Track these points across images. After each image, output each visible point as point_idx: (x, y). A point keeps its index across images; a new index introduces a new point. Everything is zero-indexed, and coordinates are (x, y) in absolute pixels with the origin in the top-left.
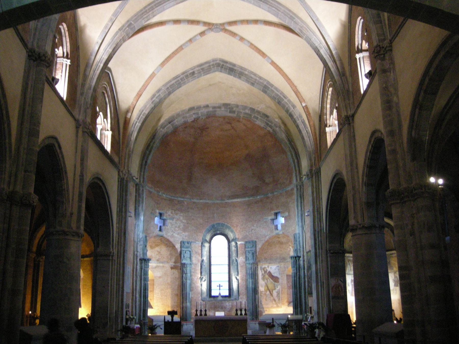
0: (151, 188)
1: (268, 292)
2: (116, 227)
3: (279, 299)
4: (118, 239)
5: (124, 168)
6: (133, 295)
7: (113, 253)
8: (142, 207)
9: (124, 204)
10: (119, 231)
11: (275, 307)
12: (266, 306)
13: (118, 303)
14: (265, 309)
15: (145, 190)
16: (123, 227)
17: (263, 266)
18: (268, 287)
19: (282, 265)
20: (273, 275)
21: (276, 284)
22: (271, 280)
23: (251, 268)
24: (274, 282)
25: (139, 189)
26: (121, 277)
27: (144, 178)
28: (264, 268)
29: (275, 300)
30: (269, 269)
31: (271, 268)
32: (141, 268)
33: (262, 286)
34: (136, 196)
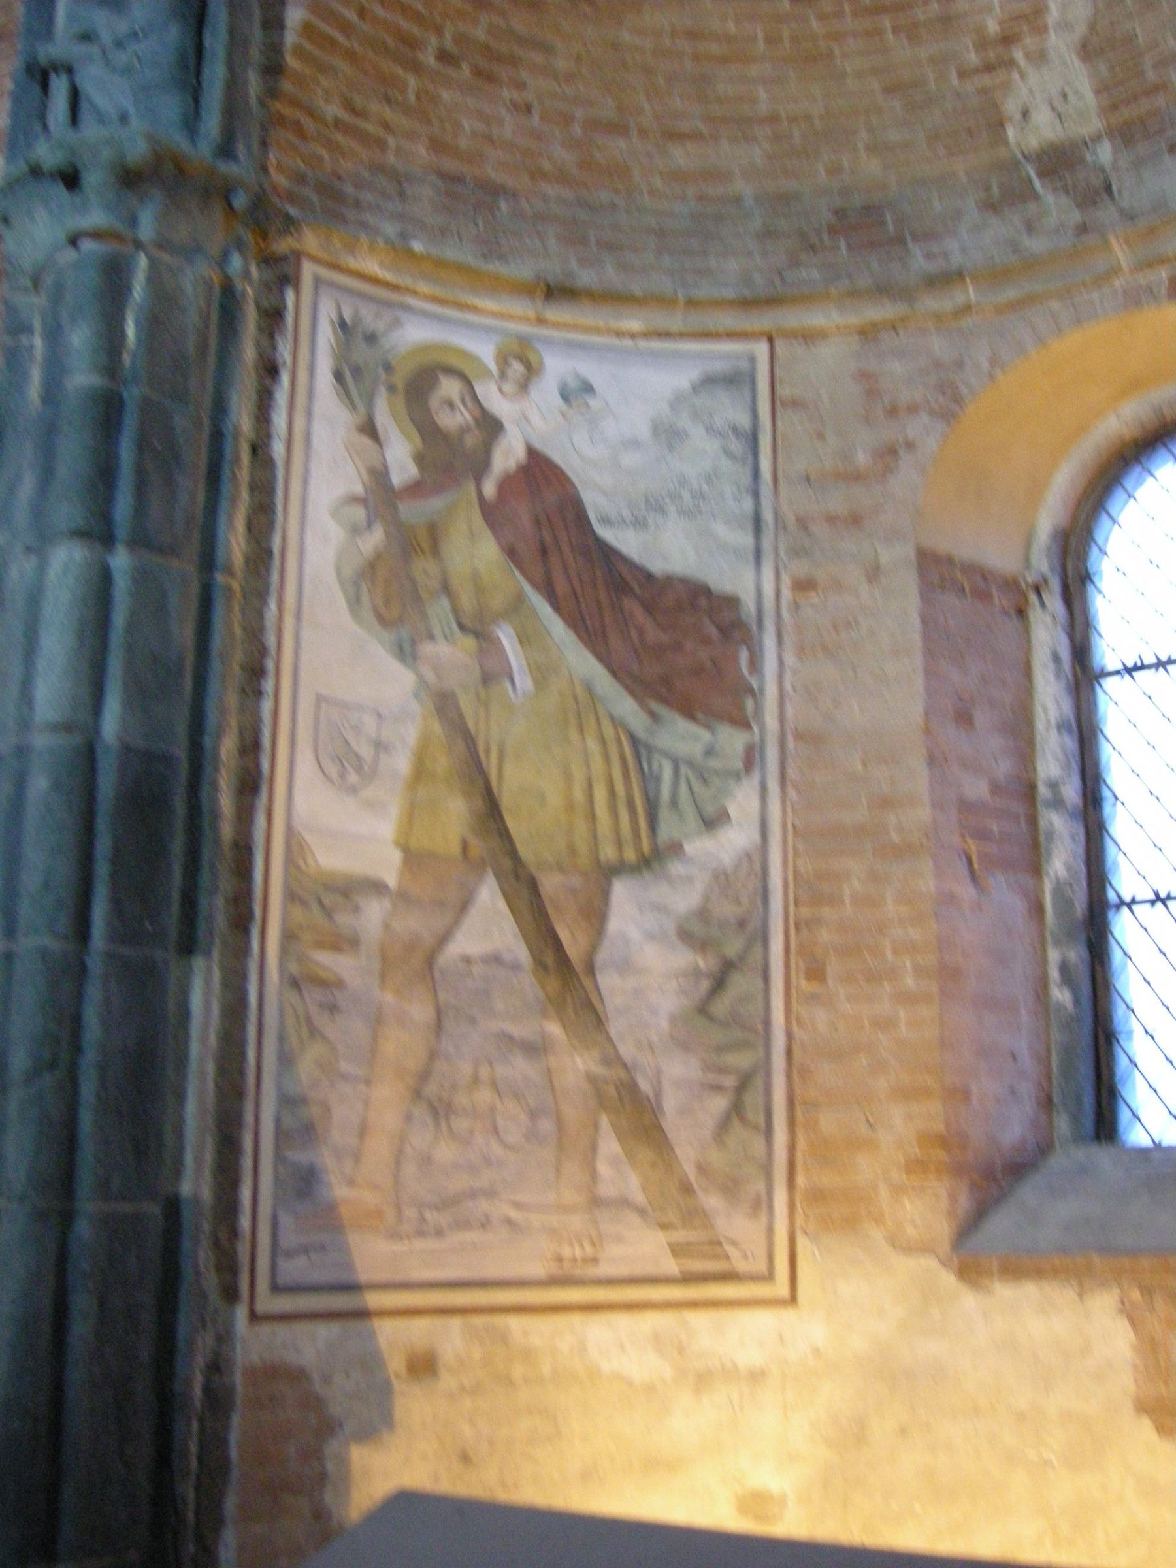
1: (488, 927)
3: (742, 1100)
11: (627, 1293)
12: (418, 1259)
14: (394, 1337)
17: (414, 334)
18: (490, 813)
19: (828, 342)
20: (627, 542)
21: (681, 736)
22: (580, 661)
23: (114, 275)
24: (626, 707)
28: (419, 385)
29: (638, 1115)
30: (528, 421)
31: (576, 393)
33: (349, 767)
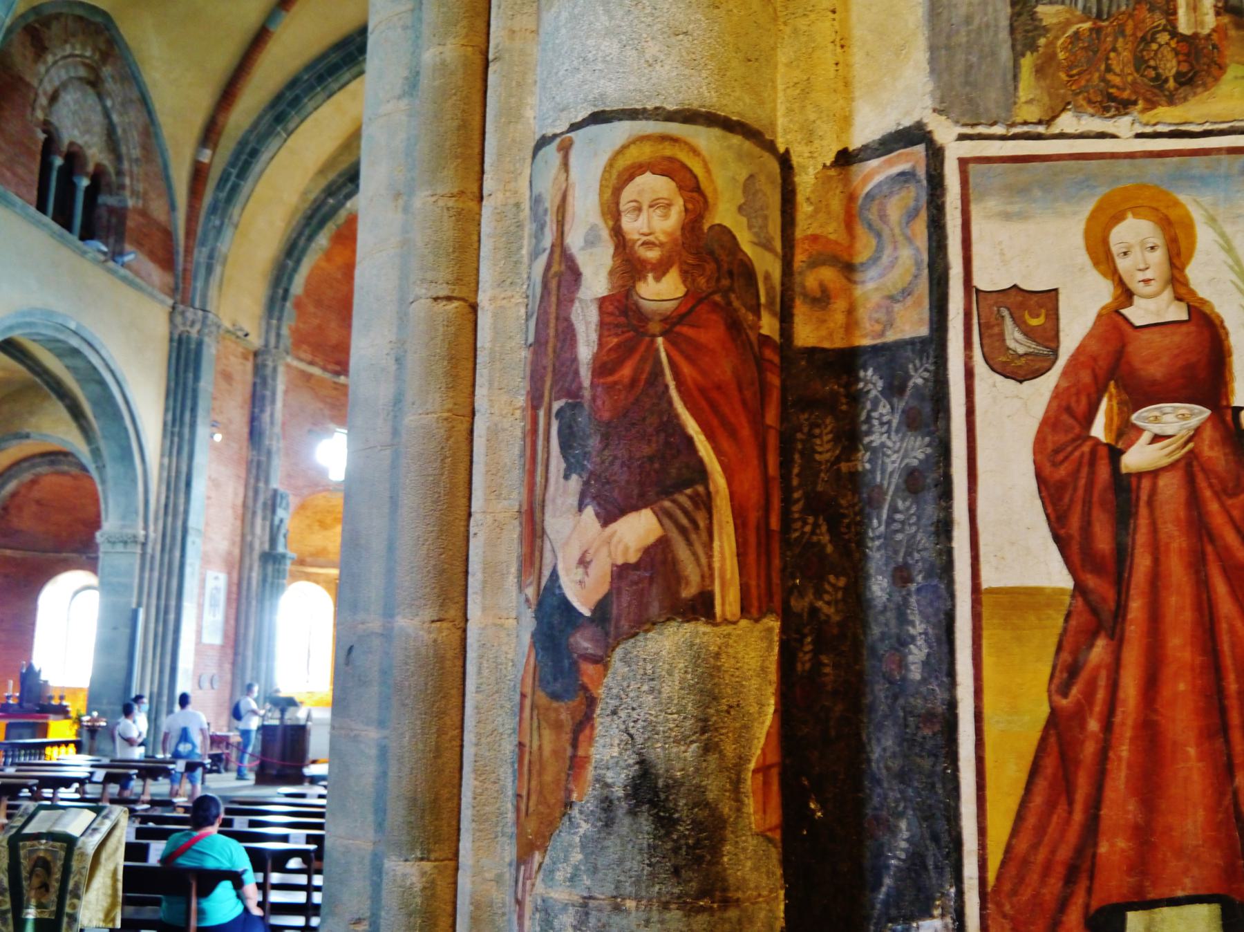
0: (311, 363)
2: (161, 465)
4: (167, 497)
5: (193, 306)
6: (236, 654)
7: (146, 537)
8: (272, 415)
9: (189, 403)
10: (169, 476)
13: (161, 672)
15: (281, 369)
16: (184, 469)
25: (265, 366)
26: (173, 603)
27: (278, 335)
32: (264, 580)
34: (255, 384)
